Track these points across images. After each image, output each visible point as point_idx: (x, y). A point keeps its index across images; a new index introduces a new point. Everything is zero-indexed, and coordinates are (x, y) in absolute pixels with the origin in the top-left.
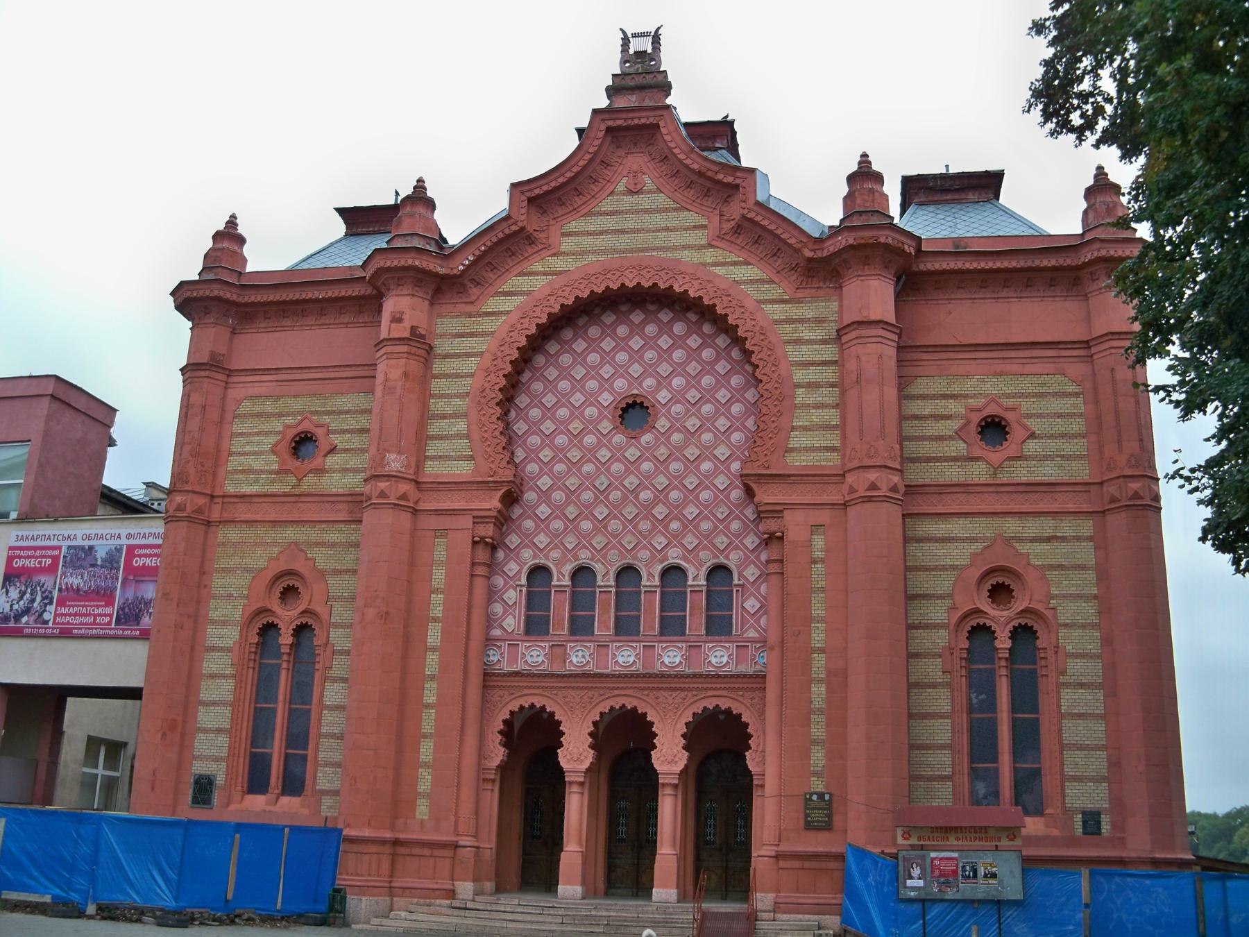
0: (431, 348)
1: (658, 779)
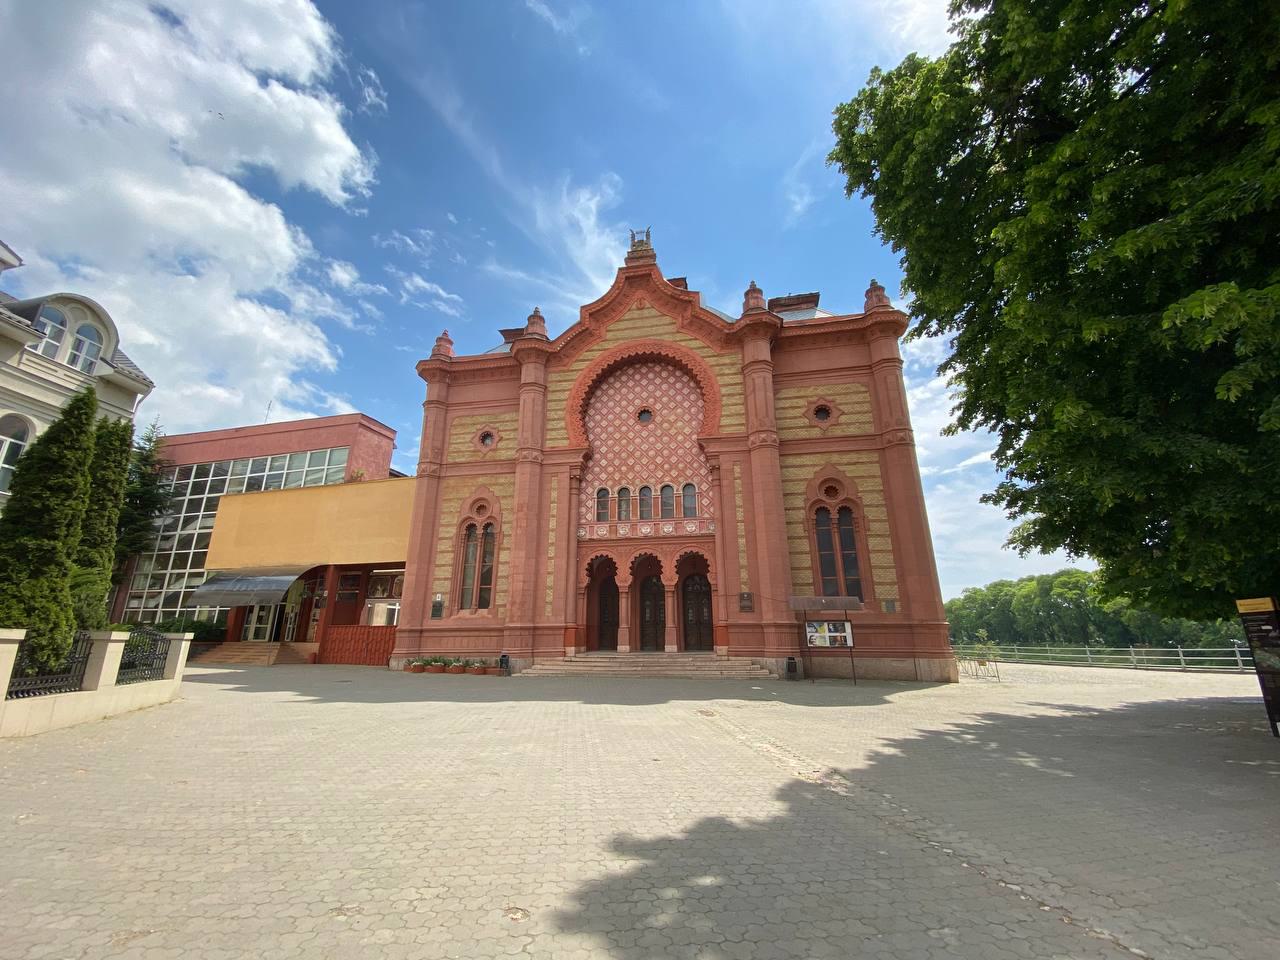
0: (546, 387)
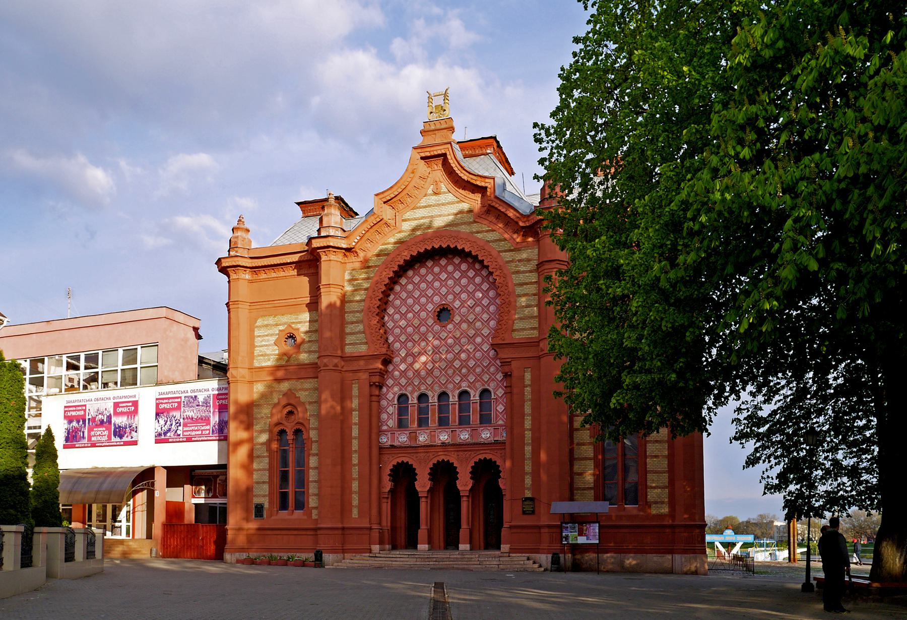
1: (459, 493)
